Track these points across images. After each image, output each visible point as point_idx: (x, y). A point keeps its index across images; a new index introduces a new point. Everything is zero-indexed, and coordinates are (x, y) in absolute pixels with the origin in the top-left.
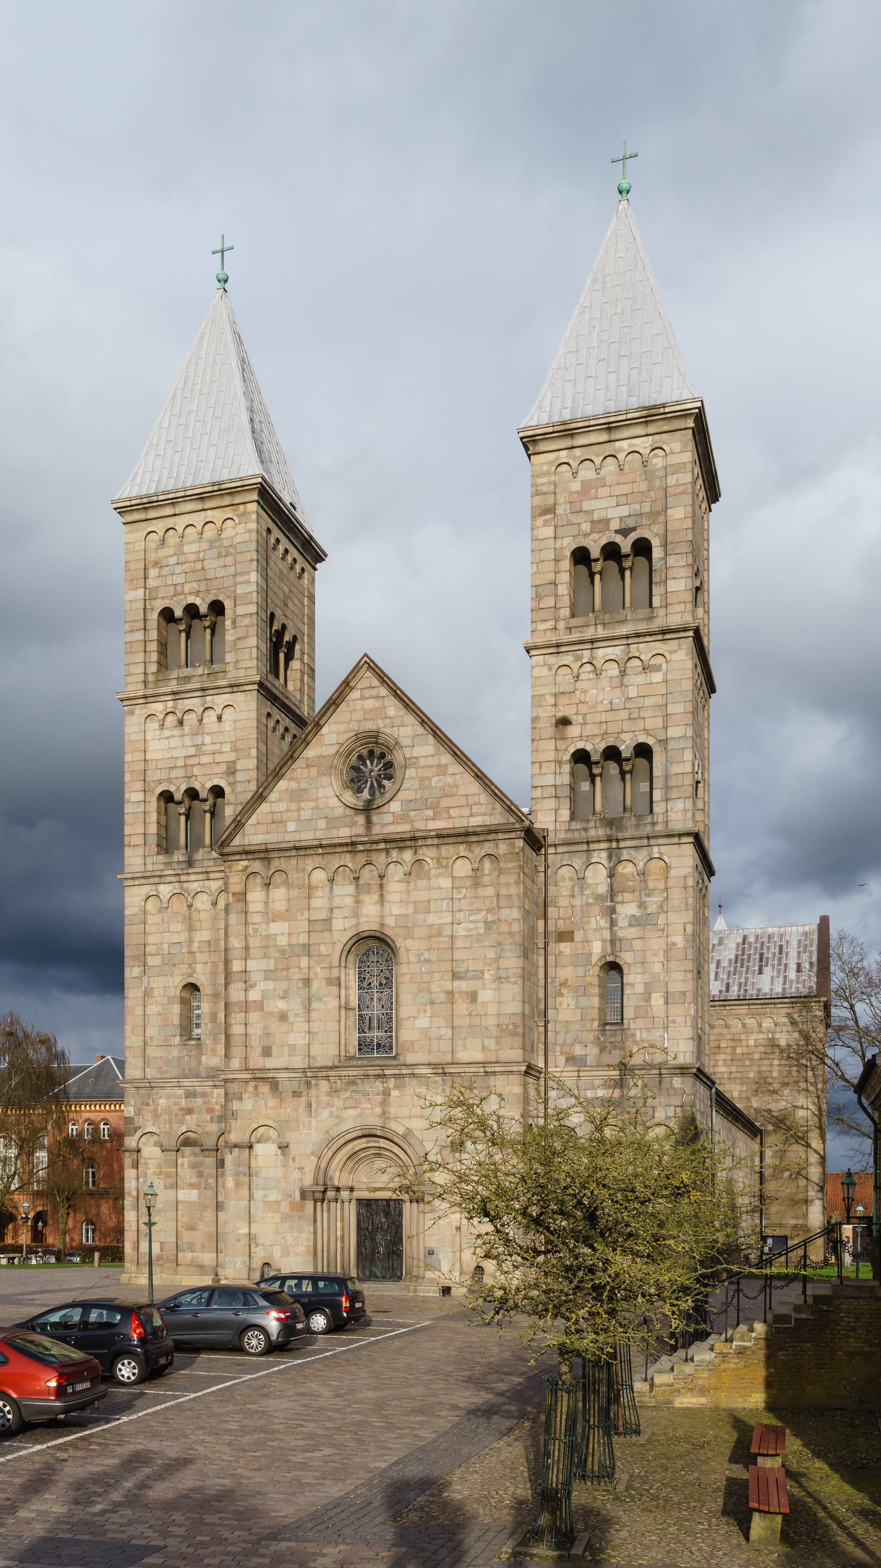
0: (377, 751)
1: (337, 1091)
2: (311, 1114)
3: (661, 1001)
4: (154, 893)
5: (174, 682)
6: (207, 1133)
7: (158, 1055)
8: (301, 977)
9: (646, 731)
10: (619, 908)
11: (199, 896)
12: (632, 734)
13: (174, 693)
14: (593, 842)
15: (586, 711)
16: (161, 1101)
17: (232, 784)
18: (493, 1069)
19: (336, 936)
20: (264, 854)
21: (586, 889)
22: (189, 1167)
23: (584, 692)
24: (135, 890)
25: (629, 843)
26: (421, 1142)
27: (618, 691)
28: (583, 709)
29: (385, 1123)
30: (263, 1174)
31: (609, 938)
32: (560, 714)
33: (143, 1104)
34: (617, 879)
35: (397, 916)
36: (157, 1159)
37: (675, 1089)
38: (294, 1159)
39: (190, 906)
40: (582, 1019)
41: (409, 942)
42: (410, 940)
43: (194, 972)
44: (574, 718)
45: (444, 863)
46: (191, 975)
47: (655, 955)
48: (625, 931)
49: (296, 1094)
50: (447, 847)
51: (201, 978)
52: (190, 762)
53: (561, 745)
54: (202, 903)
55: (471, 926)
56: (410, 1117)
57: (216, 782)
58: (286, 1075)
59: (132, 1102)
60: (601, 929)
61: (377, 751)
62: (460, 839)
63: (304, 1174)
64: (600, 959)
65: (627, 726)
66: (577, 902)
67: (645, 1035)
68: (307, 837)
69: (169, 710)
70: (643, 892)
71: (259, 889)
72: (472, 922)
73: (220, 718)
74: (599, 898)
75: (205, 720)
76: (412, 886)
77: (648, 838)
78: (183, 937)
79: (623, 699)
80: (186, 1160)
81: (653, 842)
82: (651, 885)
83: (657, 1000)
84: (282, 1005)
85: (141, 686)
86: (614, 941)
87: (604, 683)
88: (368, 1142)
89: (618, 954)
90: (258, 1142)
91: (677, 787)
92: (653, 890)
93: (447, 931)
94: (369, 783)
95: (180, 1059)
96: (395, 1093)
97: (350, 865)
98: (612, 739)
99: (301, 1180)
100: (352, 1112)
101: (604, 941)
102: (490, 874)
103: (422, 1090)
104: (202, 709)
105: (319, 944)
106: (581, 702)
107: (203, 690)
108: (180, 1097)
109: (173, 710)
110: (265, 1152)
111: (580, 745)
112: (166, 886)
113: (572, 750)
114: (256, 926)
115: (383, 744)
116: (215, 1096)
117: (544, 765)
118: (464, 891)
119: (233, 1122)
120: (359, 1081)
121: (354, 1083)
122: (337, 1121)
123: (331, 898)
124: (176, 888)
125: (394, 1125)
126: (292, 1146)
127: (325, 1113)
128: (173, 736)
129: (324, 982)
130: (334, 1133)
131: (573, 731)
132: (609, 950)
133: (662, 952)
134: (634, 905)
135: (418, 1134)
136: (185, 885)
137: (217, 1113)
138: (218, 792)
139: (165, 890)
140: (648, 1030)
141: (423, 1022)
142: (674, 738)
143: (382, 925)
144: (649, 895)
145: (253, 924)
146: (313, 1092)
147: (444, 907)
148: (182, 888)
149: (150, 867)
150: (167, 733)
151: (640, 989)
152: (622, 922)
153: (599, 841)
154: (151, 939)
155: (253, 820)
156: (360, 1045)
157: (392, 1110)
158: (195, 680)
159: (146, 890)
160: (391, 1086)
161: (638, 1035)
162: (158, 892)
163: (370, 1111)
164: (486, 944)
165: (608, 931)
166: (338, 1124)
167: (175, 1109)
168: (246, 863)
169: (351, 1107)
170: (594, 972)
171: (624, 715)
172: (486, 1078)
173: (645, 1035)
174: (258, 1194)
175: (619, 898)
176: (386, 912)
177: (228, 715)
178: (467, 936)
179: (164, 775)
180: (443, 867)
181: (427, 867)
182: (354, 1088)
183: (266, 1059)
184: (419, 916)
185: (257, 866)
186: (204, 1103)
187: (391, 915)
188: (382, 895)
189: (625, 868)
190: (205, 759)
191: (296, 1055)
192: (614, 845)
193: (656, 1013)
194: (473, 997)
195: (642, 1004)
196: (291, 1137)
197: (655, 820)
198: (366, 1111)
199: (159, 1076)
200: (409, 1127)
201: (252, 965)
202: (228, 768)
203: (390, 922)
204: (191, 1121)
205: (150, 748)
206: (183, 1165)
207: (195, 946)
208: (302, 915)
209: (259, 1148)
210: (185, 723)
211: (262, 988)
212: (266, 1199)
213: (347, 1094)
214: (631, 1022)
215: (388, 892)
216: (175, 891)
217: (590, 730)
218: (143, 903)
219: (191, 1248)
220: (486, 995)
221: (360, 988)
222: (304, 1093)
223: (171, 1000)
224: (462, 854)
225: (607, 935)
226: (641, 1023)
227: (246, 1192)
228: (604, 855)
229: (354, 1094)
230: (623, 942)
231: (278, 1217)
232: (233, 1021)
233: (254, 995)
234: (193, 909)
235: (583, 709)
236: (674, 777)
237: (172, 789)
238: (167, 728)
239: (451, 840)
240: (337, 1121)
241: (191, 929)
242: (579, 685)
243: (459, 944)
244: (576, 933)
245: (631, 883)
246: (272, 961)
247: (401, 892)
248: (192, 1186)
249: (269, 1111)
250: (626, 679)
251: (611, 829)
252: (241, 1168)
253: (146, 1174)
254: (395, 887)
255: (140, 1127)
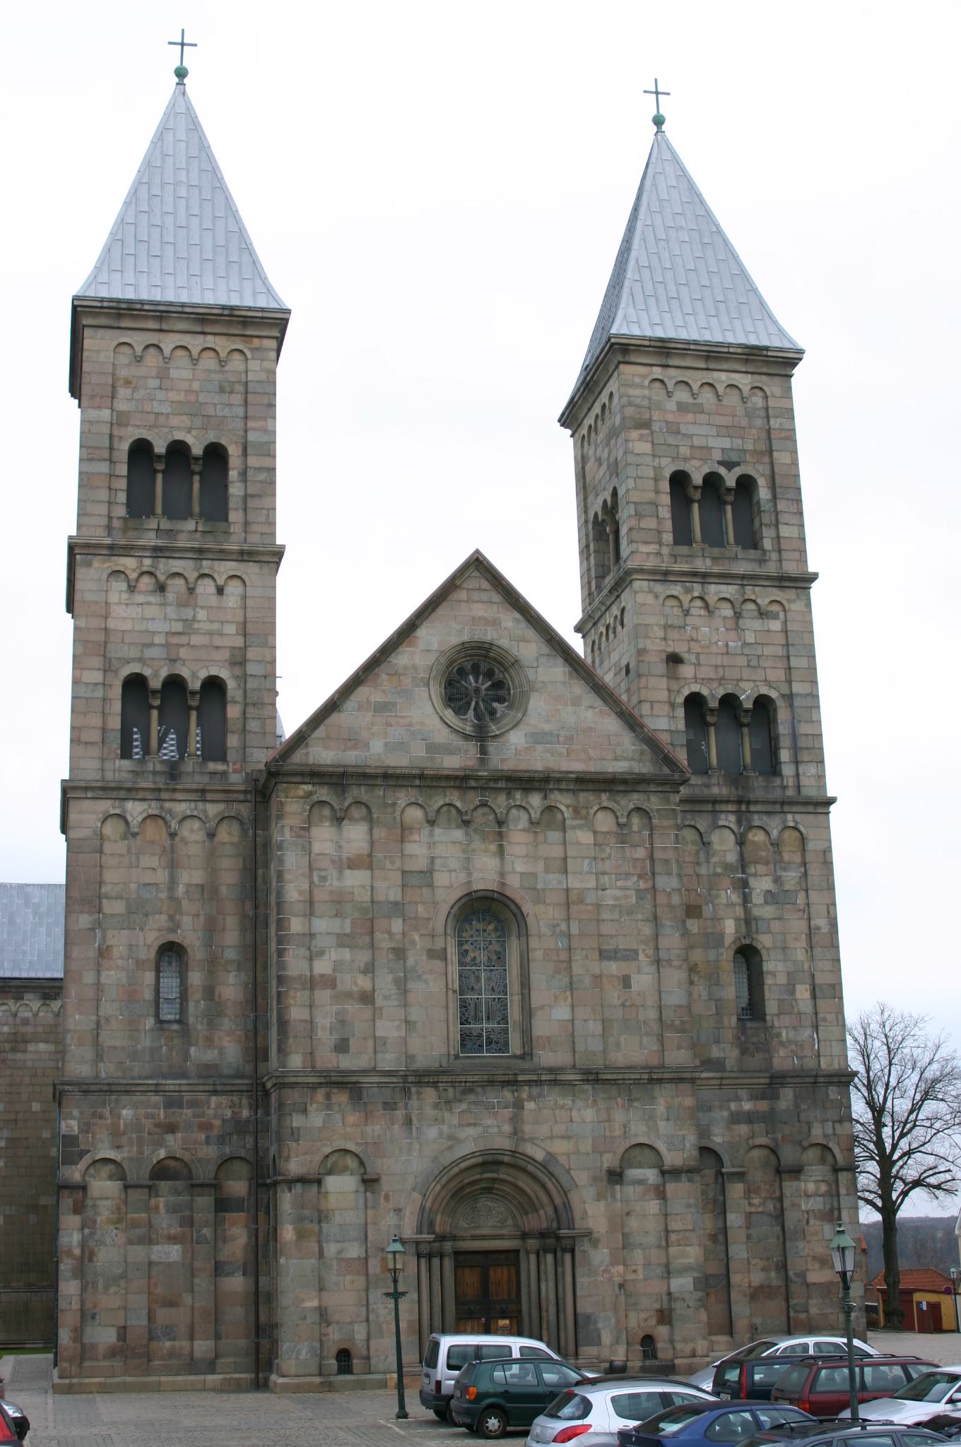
0: (484, 667)
1: (448, 1102)
2: (411, 1133)
3: (807, 995)
4: (118, 811)
5: (152, 534)
6: (200, 1160)
7: (118, 1044)
8: (393, 945)
9: (768, 683)
10: (752, 881)
11: (188, 823)
12: (752, 684)
13: (156, 549)
14: (721, 802)
15: (699, 650)
16: (124, 1112)
17: (243, 678)
18: (660, 1076)
19: (440, 894)
20: (338, 779)
21: (713, 856)
22: (168, 1211)
23: (696, 629)
24: (86, 805)
25: (760, 808)
26: (568, 1171)
27: (733, 634)
28: (696, 647)
29: (517, 1145)
30: (337, 1219)
31: (742, 916)
32: (670, 650)
33: (94, 1115)
34: (748, 849)
35: (522, 874)
36: (113, 1199)
37: (832, 1101)
38: (387, 1197)
39: (173, 835)
40: (717, 1014)
41: (540, 909)
42: (541, 906)
43: (178, 926)
44: (685, 656)
45: (584, 812)
46: (173, 930)
47: (797, 939)
48: (764, 911)
49: (389, 1106)
50: (585, 794)
51: (190, 935)
52: (175, 640)
53: (675, 686)
54: (192, 833)
55: (619, 893)
56: (552, 1138)
57: (214, 671)
58: (376, 1079)
59: (76, 1113)
60: (733, 905)
61: (484, 667)
62: (602, 786)
63: (401, 1219)
64: (734, 942)
65: (746, 673)
66: (703, 870)
67: (792, 1034)
68: (399, 761)
69: (145, 569)
70: (778, 866)
71: (327, 824)
72: (620, 888)
73: (220, 591)
74: (728, 867)
75: (199, 590)
76: (541, 837)
77: (783, 803)
78: (162, 876)
79: (740, 644)
80: (162, 1199)
81: (786, 808)
82: (786, 857)
83: (803, 992)
84: (364, 982)
85: (101, 532)
86: (748, 921)
87: (718, 622)
88: (484, 1172)
89: (755, 936)
90: (330, 1173)
91: (807, 748)
92: (789, 863)
93: (591, 898)
94: (473, 704)
95: (154, 1051)
96: (530, 1106)
97: (458, 804)
98: (730, 686)
99: (399, 1227)
100: (471, 1131)
101: (737, 920)
102: (640, 832)
103: (566, 1102)
104: (196, 574)
105: (416, 903)
106: (692, 640)
107: (200, 551)
108: (156, 1106)
109: (152, 570)
110: (341, 1186)
111: (695, 688)
112: (137, 803)
113: (686, 692)
114: (323, 873)
115: (495, 660)
116: (213, 1105)
117: (656, 706)
118: (608, 850)
119: (293, 1144)
120: (479, 1089)
121: (471, 1091)
122: (450, 1143)
123: (431, 845)
124: (154, 808)
125: (530, 1150)
126: (384, 1179)
127: (432, 1132)
128: (149, 604)
129: (425, 953)
130: (447, 1159)
131: (686, 671)
132: (744, 930)
133: (804, 936)
134: (769, 879)
135: (562, 1160)
136: (167, 805)
137: (215, 1132)
138: (214, 686)
139: (135, 810)
140: (794, 1028)
141: (562, 1013)
142: (801, 695)
143: (503, 884)
144: (785, 869)
145: (320, 869)
146: (414, 1102)
147: (586, 868)
148: (162, 808)
149: (109, 776)
150: (140, 598)
151: (782, 979)
152: (757, 899)
153: (728, 802)
154: (109, 876)
155: (320, 732)
156: (463, 1039)
157: (527, 1128)
158: (182, 537)
159: (105, 806)
160: (524, 1096)
161: (784, 1035)
162: (125, 811)
163: (496, 1130)
164: (640, 917)
165: (742, 908)
166: (450, 1148)
167: (148, 1124)
168: (308, 788)
169: (469, 1125)
170: (727, 955)
171: (742, 661)
172: (649, 1086)
173: (792, 1034)
174: (331, 1249)
175: (752, 870)
176: (508, 868)
177: (233, 589)
178: (614, 906)
179: (134, 653)
180: (581, 818)
181: (559, 816)
182: (472, 1097)
183: (341, 1056)
184: (551, 876)
185: (324, 793)
186: (195, 1116)
187: (514, 872)
188: (501, 846)
189: (755, 835)
190: (196, 640)
191: (387, 1052)
192: (744, 808)
193: (802, 1009)
194: (626, 982)
195: (785, 997)
196: (378, 1165)
197: (785, 783)
198: (490, 1130)
199: (119, 1074)
200: (550, 1150)
201: (320, 925)
202: (232, 655)
203: (514, 881)
204: (174, 1143)
205: (113, 614)
206: (157, 1208)
207: (181, 890)
208: (393, 863)
209: (332, 1182)
210: (169, 589)
211: (334, 957)
212: (342, 1256)
213: (464, 1106)
214: (775, 1019)
215: (509, 843)
216: (151, 812)
217: (705, 672)
218: (99, 825)
219: (170, 1333)
220: (643, 980)
221: (461, 964)
222: (401, 1104)
223: (140, 964)
224: (605, 804)
225: (739, 912)
226: (786, 1020)
227: (314, 1246)
228: (732, 818)
229: (472, 1107)
230: (760, 923)
231: (360, 1282)
232: (292, 1002)
233: (322, 967)
234: (177, 839)
235: (696, 647)
236: (804, 738)
237: (147, 672)
238: (140, 592)
239: (590, 786)
240: (450, 1143)
241: (173, 865)
242: (689, 620)
243: (605, 915)
244: (704, 908)
245: (764, 854)
246: (348, 922)
247: (527, 844)
248: (172, 1239)
249: (349, 1130)
250: (741, 622)
251: (737, 788)
252: (306, 1212)
253: (95, 1222)
254: (518, 838)
255: (89, 1151)
